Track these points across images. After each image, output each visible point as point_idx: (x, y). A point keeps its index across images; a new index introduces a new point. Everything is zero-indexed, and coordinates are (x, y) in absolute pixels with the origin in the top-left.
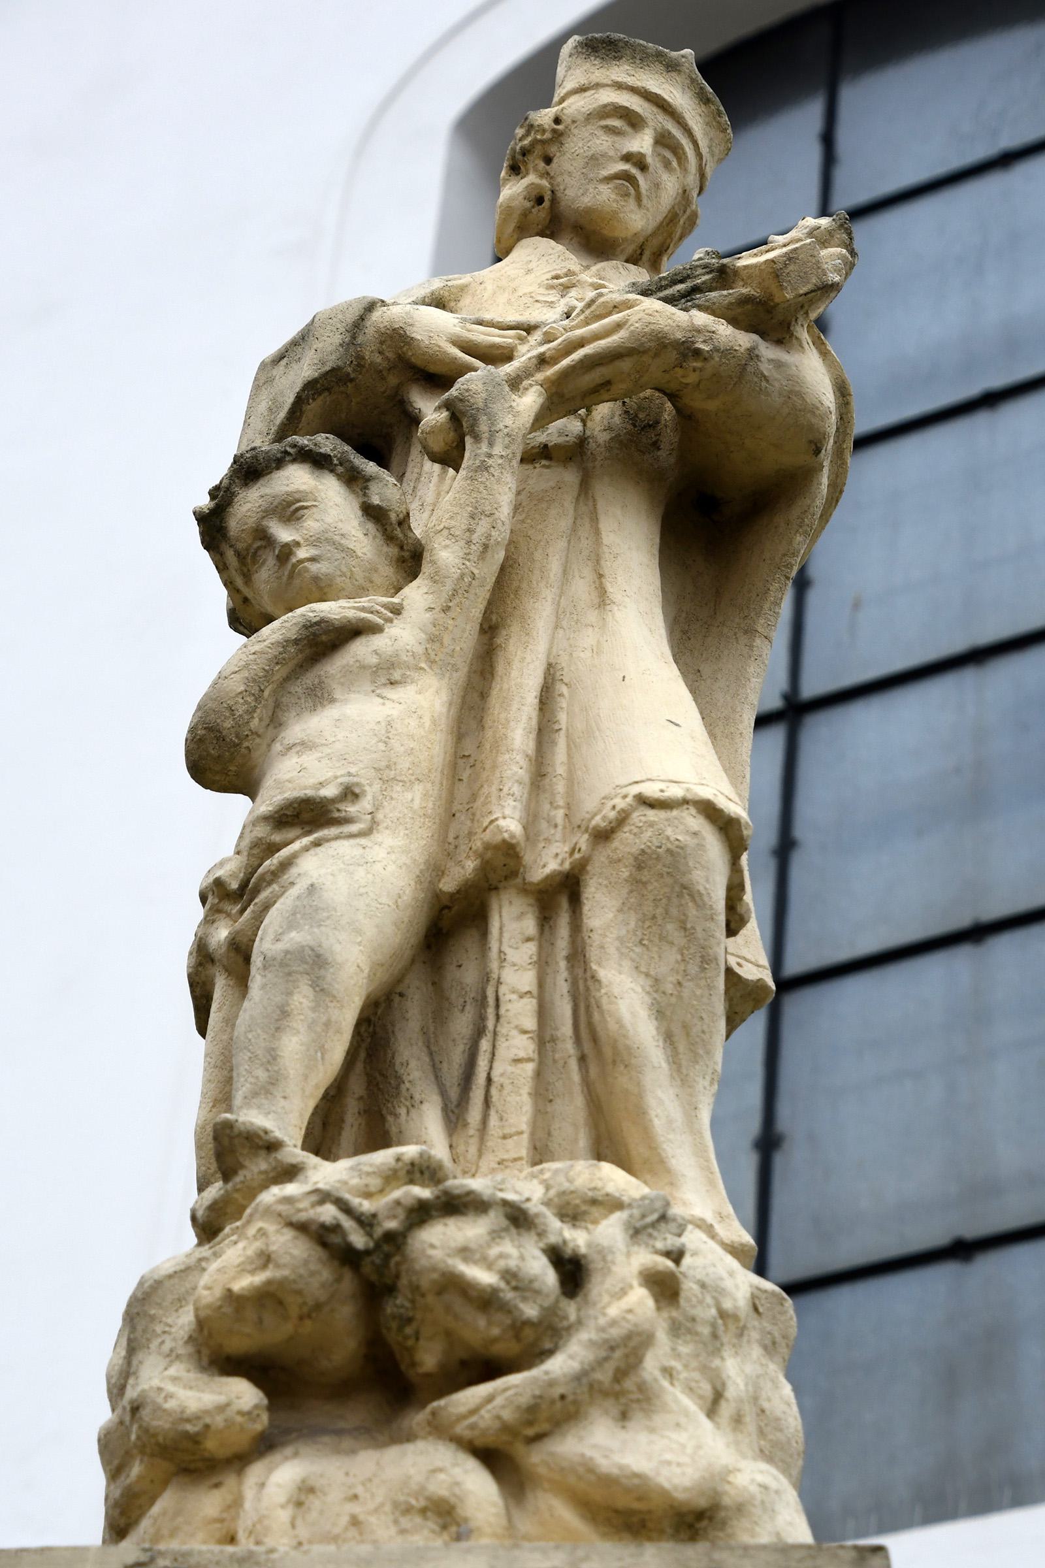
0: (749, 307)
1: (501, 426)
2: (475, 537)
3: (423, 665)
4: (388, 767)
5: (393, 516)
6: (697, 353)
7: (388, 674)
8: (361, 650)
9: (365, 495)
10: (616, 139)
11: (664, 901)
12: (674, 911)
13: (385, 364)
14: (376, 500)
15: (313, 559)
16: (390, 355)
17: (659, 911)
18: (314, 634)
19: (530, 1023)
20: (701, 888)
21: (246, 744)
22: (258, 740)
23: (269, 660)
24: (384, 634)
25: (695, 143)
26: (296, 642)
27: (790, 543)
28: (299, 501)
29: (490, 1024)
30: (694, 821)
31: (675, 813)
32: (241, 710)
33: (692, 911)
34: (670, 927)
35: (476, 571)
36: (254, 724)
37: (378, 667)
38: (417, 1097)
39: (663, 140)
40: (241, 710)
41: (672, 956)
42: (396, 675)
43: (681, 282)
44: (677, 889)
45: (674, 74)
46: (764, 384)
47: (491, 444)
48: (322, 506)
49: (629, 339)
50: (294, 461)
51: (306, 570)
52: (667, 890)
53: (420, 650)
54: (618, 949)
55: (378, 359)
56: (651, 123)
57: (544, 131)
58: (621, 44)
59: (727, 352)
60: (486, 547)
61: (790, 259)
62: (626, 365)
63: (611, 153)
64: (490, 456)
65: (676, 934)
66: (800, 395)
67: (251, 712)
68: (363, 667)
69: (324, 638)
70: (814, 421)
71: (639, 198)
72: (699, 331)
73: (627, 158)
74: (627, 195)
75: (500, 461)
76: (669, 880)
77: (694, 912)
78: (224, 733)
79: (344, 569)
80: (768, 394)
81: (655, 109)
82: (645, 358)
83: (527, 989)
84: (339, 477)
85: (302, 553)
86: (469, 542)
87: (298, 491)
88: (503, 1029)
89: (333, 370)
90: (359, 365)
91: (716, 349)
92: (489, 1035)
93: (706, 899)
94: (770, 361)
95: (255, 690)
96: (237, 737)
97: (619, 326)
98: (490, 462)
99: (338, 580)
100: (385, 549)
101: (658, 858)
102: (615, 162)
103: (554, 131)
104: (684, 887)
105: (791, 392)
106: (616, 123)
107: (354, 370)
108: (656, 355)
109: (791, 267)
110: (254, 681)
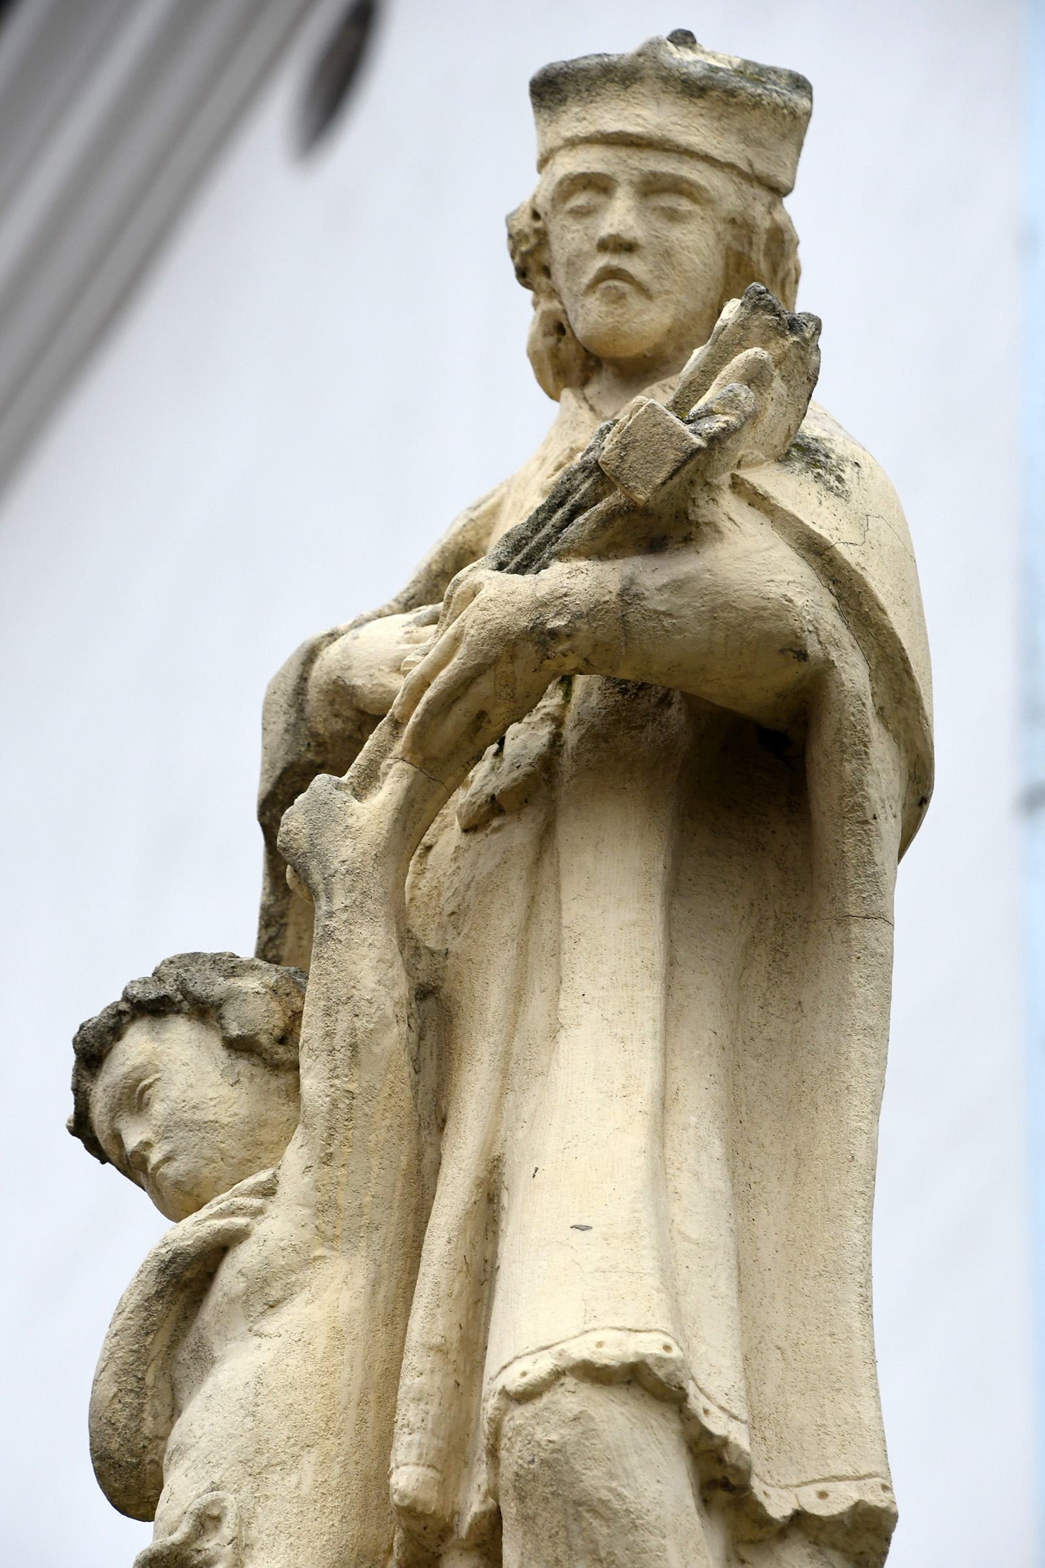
0: (619, 522)
2: (338, 1042)
3: (318, 1252)
5: (264, 1039)
6: (554, 634)
7: (266, 1295)
8: (230, 1277)
9: (223, 1028)
10: (587, 221)
11: (562, 1533)
12: (578, 1542)
13: (350, 726)
14: (234, 1031)
15: (168, 1159)
16: (348, 713)
17: (561, 1548)
18: (174, 1276)
20: (604, 1495)
23: (135, 1335)
24: (252, 1239)
25: (707, 159)
26: (159, 1295)
27: (841, 778)
28: (141, 1080)
30: (572, 1399)
31: (546, 1398)
32: (122, 1419)
33: (601, 1530)
35: (352, 1087)
39: (650, 188)
40: (122, 1419)
43: (561, 504)
44: (571, 1511)
45: (636, 87)
46: (667, 622)
47: (329, 898)
48: (166, 1076)
49: (468, 656)
50: (133, 1019)
51: (165, 1177)
52: (558, 1517)
53: (307, 1234)
55: (338, 725)
56: (622, 178)
57: (526, 237)
58: (561, 79)
59: (594, 612)
60: (354, 1047)
61: (625, 447)
62: (484, 686)
63: (586, 247)
64: (330, 915)
66: (728, 606)
68: (232, 1301)
69: (188, 1274)
70: (766, 627)
71: (643, 290)
72: (545, 605)
73: (604, 246)
74: (621, 297)
75: (344, 916)
76: (557, 1503)
78: (116, 1456)
79: (208, 1153)
80: (681, 631)
81: (623, 153)
82: (503, 668)
84: (189, 1016)
85: (155, 1157)
86: (331, 1052)
87: (135, 1068)
89: (285, 771)
90: (319, 745)
93: (616, 1505)
95: (132, 1383)
96: (132, 1456)
97: (457, 640)
98: (333, 923)
99: (205, 1172)
100: (274, 1083)
101: (535, 1478)
102: (593, 257)
103: (537, 231)
104: (578, 1503)
105: (713, 610)
106: (580, 200)
107: (317, 753)
108: (513, 658)
109: (632, 457)
110: (126, 1372)
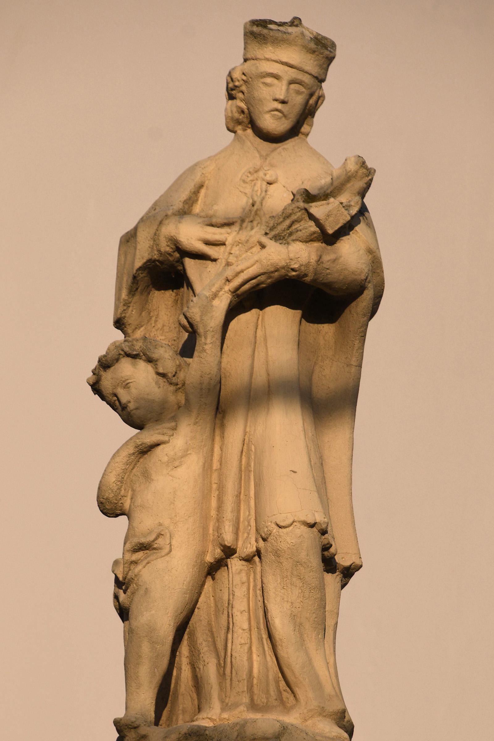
1: (209, 328)
4: (176, 516)
7: (174, 463)
12: (295, 573)
14: (161, 370)
17: (289, 574)
19: (246, 626)
21: (120, 502)
22: (125, 498)
23: (124, 464)
26: (134, 454)
29: (231, 627)
32: (116, 488)
34: (294, 579)
36: (123, 492)
37: (168, 462)
38: (206, 661)
41: (297, 591)
42: (177, 463)
46: (328, 271)
47: (206, 338)
54: (275, 593)
65: (298, 582)
67: (119, 489)
77: (304, 571)
83: (243, 609)
88: (236, 629)
91: (301, 265)
92: (231, 633)
94: (328, 261)
96: (116, 500)
